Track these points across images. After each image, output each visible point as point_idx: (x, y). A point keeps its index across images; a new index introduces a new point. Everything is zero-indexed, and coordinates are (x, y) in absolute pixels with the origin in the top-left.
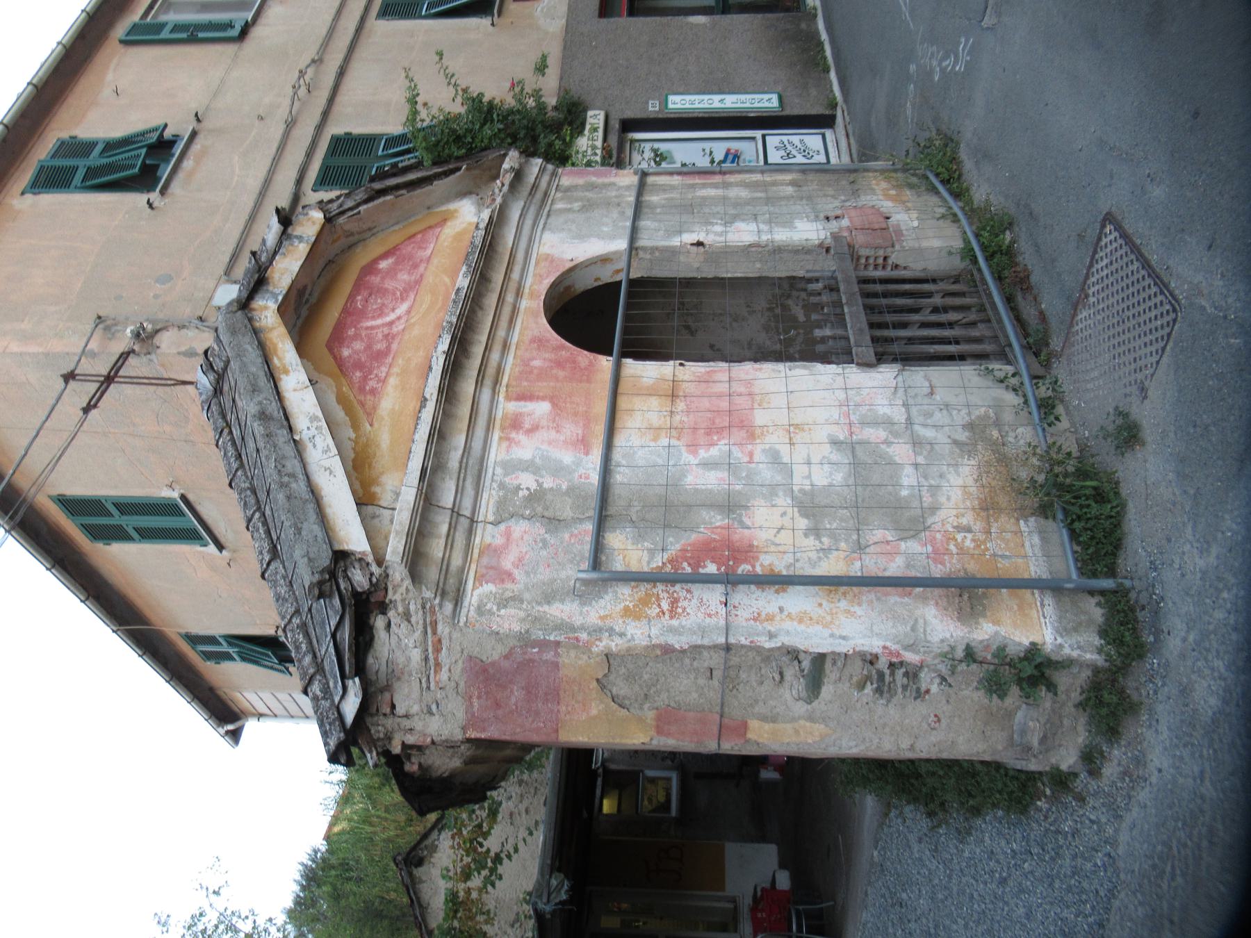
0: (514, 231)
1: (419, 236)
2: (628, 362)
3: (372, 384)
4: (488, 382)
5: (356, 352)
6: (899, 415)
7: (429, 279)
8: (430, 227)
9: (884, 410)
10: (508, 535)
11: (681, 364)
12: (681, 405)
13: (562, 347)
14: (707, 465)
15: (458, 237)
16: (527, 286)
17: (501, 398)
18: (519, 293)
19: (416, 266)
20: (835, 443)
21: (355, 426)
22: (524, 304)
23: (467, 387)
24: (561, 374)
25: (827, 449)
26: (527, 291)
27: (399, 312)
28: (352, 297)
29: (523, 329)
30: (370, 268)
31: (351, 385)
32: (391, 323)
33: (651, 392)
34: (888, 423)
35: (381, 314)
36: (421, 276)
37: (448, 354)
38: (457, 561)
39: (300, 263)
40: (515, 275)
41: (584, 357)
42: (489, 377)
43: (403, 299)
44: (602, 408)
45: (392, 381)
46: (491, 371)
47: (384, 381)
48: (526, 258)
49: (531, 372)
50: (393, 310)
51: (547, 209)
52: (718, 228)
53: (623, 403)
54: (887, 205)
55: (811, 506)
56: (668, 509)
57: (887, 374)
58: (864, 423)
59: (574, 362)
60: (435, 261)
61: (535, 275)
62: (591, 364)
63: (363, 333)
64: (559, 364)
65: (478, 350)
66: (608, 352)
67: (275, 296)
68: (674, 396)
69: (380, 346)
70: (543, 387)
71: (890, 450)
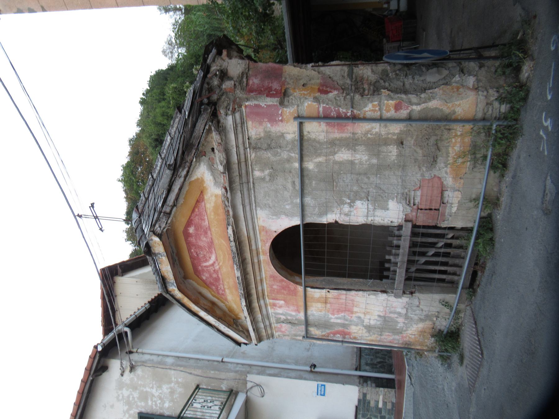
0: (244, 223)
1: (197, 210)
2: (309, 289)
3: (221, 292)
4: (261, 298)
5: (207, 278)
6: (404, 311)
7: (216, 242)
8: (198, 201)
9: (399, 310)
10: (281, 326)
11: (328, 292)
12: (328, 305)
13: (282, 281)
14: (337, 318)
15: (216, 208)
16: (260, 247)
17: (267, 299)
18: (258, 254)
19: (206, 233)
20: (379, 316)
21: (222, 302)
22: (262, 257)
23: (255, 304)
24: (285, 292)
25: (376, 317)
26: (260, 250)
27: (213, 258)
28: (189, 250)
29: (265, 271)
30: (187, 235)
31: (213, 291)
32: (213, 265)
33: (318, 300)
34: (399, 314)
35: (206, 261)
36: (212, 239)
37: (246, 306)
38: (269, 332)
39: (169, 267)
40: (254, 247)
41: (292, 285)
42: (261, 296)
43: (211, 253)
44: (302, 303)
45: (227, 291)
46: (261, 294)
47: (224, 290)
48: (256, 242)
49: (274, 291)
50: (210, 258)
51: (251, 180)
52: (346, 208)
53: (308, 304)
54: (449, 181)
55: (369, 328)
56: (326, 325)
57: (405, 300)
58: (391, 312)
59: (289, 288)
60: (213, 229)
61: (261, 240)
62: (295, 289)
63: (205, 269)
64: (283, 288)
65: (254, 291)
66: (302, 286)
67: (173, 284)
68: (326, 303)
69: (215, 276)
70: (279, 296)
71: (397, 319)
